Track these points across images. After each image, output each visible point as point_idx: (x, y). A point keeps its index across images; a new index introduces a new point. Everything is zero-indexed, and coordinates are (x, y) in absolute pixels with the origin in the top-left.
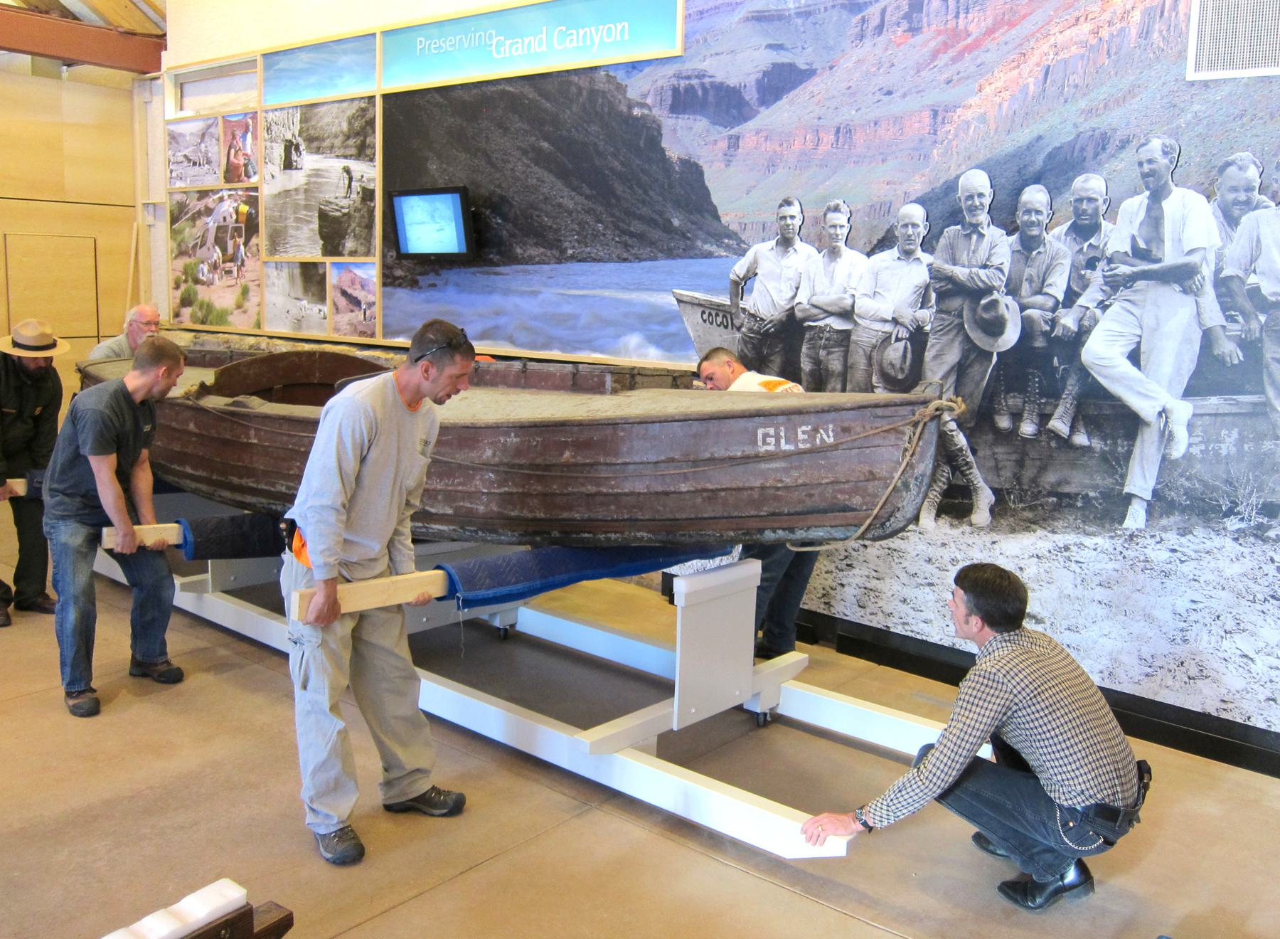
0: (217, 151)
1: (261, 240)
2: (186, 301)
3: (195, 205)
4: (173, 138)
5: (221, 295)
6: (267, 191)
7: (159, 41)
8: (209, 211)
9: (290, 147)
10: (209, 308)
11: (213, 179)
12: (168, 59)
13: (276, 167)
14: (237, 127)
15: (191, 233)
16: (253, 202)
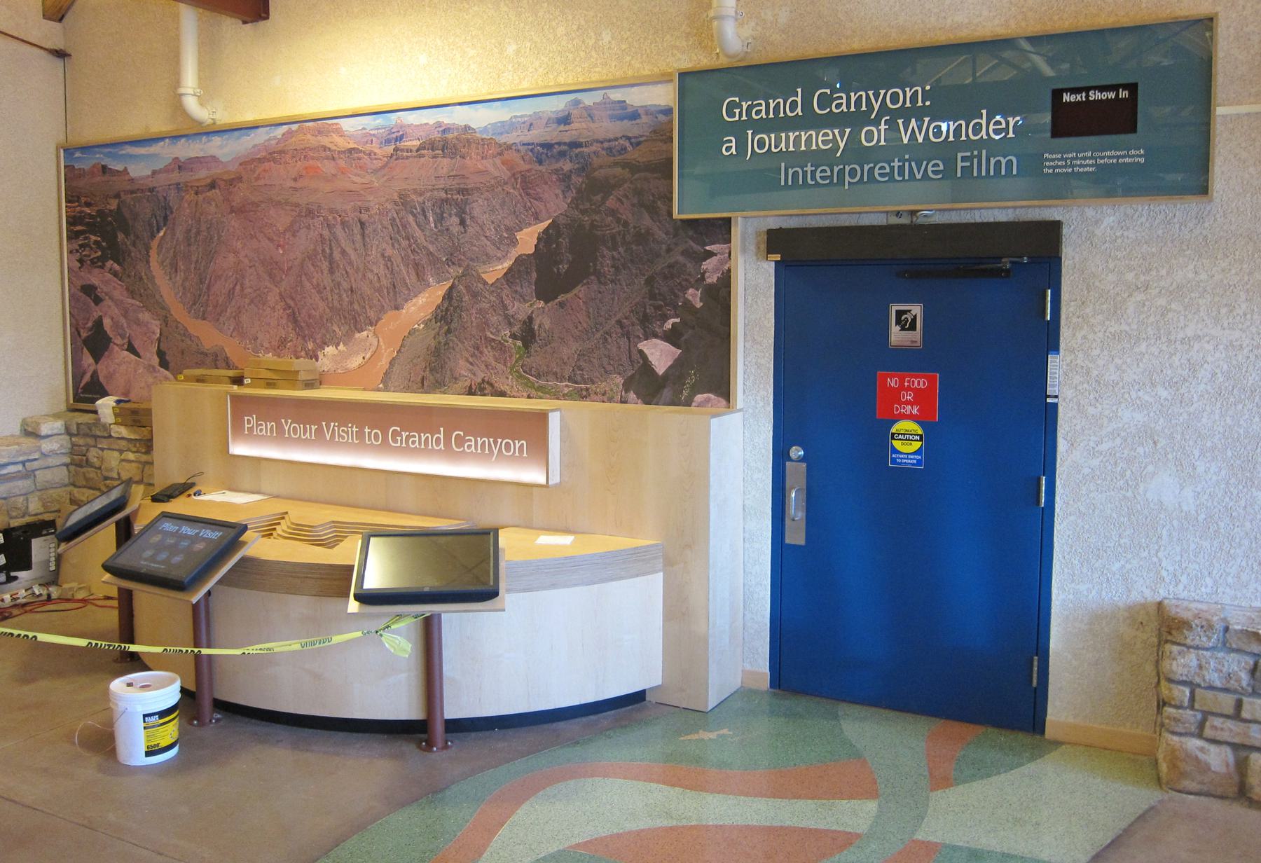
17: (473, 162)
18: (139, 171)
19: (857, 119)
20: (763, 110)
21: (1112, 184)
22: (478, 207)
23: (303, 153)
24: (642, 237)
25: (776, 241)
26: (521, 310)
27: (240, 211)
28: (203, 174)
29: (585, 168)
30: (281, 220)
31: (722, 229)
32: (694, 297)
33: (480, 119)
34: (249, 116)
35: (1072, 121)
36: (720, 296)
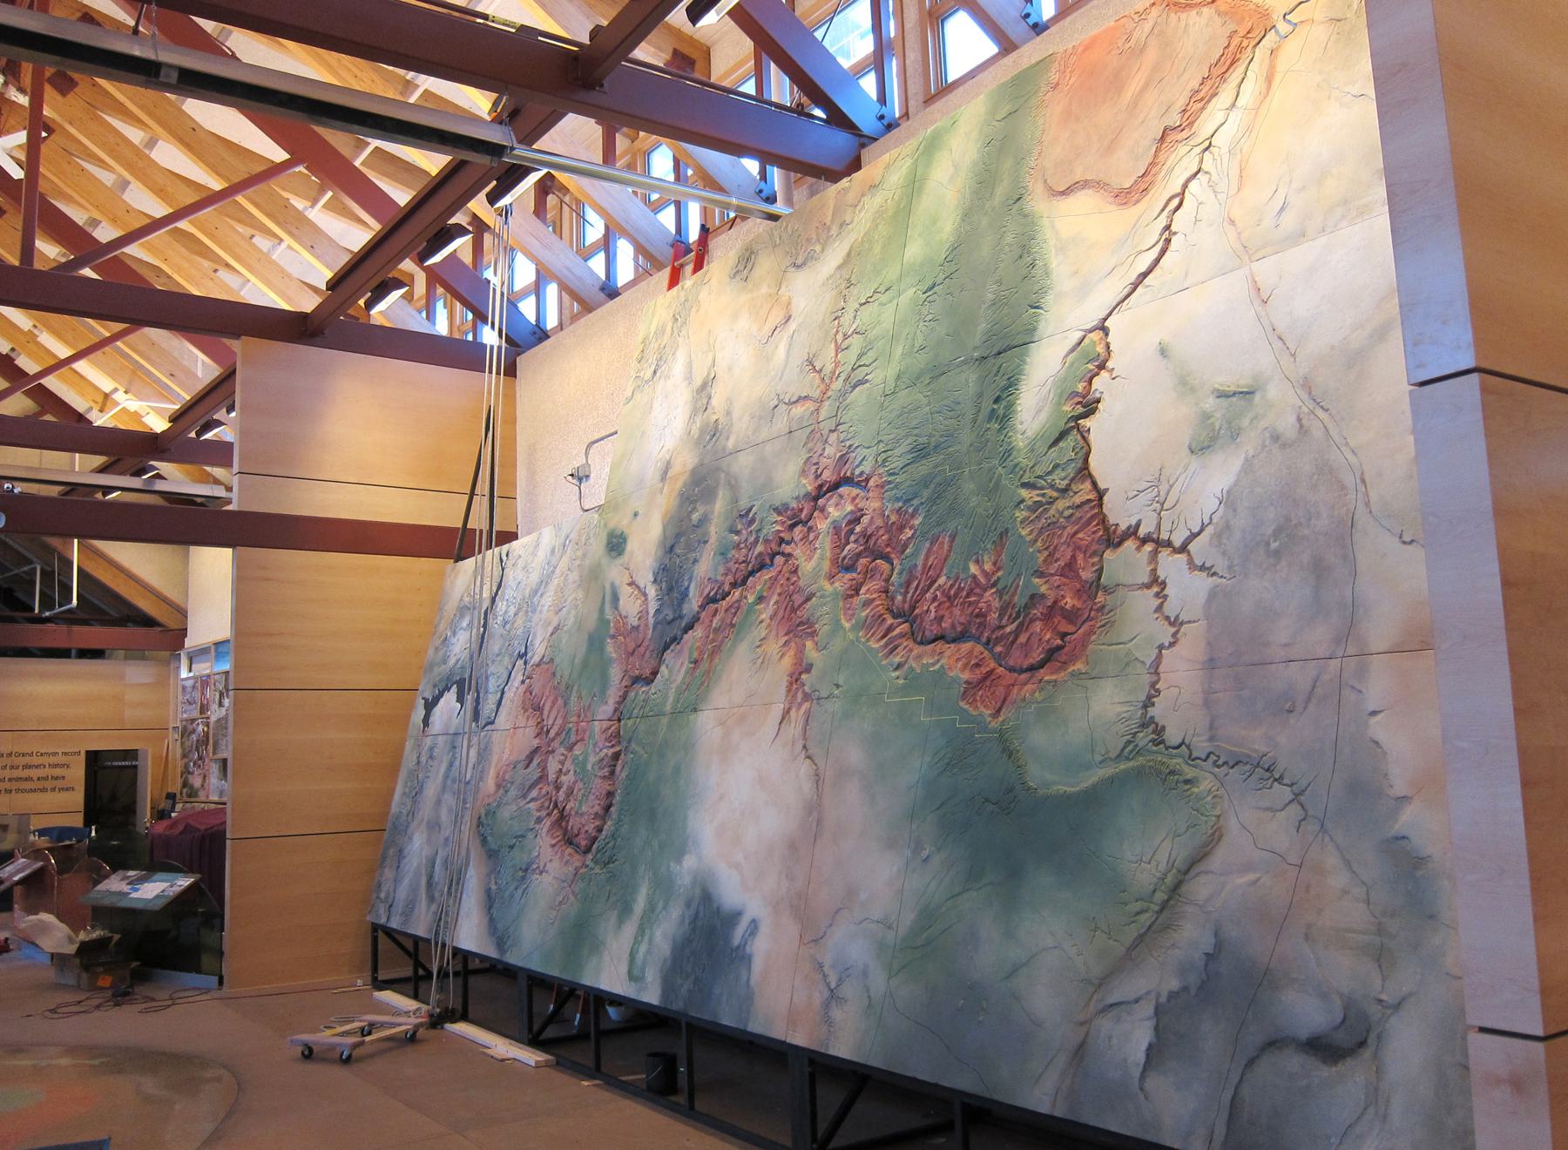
0: (197, 695)
1: (210, 748)
2: (185, 784)
3: (190, 728)
4: (184, 688)
5: (196, 781)
6: (213, 719)
7: (183, 632)
8: (194, 731)
9: (221, 694)
10: (192, 787)
11: (195, 714)
12: (189, 643)
13: (215, 707)
14: (204, 681)
15: (188, 744)
16: (208, 725)
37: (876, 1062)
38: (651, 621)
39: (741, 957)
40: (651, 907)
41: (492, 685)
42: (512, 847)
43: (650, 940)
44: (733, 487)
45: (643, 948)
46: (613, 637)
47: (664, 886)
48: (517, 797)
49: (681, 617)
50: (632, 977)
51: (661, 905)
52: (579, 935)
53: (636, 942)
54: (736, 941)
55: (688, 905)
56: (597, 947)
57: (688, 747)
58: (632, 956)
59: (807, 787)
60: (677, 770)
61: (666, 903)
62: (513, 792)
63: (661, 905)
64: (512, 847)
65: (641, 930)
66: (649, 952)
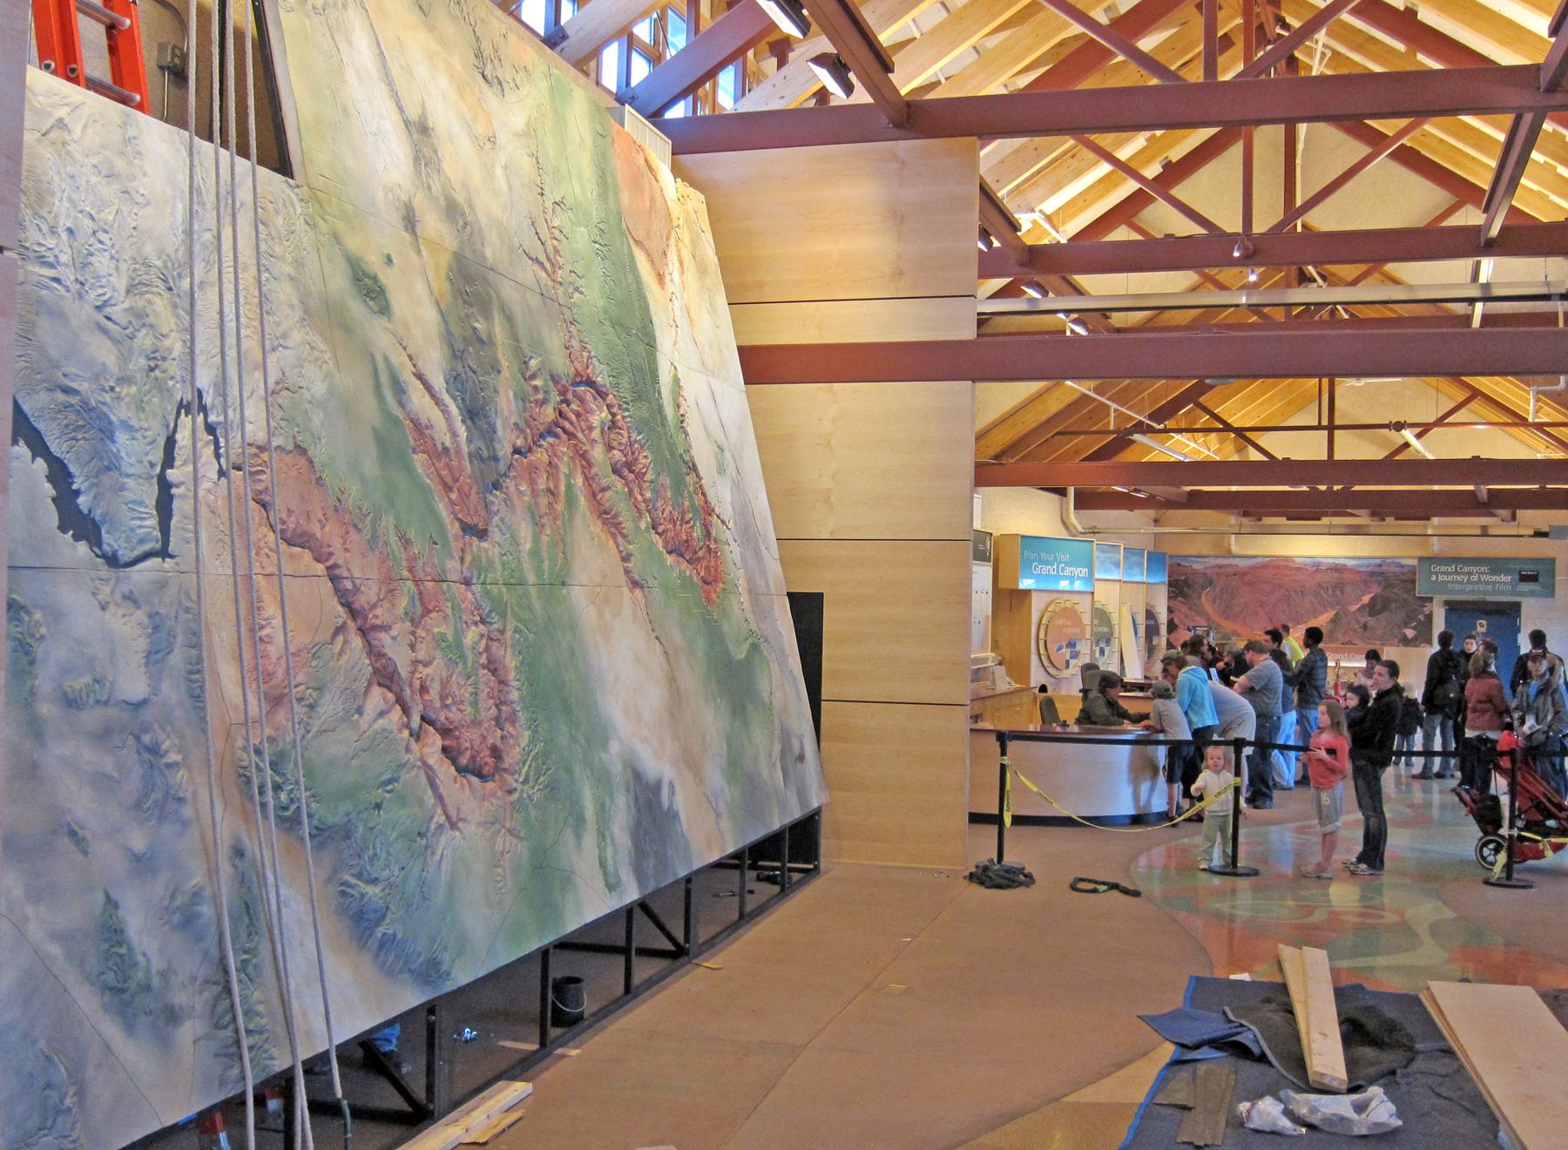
17: (1347, 576)
18: (1195, 566)
19: (1470, 574)
20: (1443, 569)
21: (1532, 594)
22: (1348, 589)
23: (1278, 567)
24: (1405, 600)
25: (1446, 603)
26: (1363, 620)
27: (1249, 584)
28: (1230, 570)
29: (1386, 580)
30: (1267, 588)
31: (1430, 600)
32: (1421, 617)
33: (1350, 563)
34: (1251, 553)
35: (1524, 578)
36: (1429, 617)
37: (740, 845)
38: (465, 449)
39: (672, 816)
40: (602, 809)
41: (135, 451)
42: (378, 806)
43: (612, 839)
44: (509, 318)
45: (609, 853)
46: (414, 451)
47: (602, 779)
48: (346, 718)
49: (495, 459)
50: (611, 887)
51: (608, 800)
52: (544, 878)
53: (602, 850)
54: (666, 804)
55: (628, 790)
56: (567, 881)
57: (573, 626)
58: (603, 865)
59: (664, 662)
60: (572, 653)
61: (612, 801)
62: (330, 706)
63: (608, 800)
64: (378, 806)
65: (601, 835)
66: (616, 853)
